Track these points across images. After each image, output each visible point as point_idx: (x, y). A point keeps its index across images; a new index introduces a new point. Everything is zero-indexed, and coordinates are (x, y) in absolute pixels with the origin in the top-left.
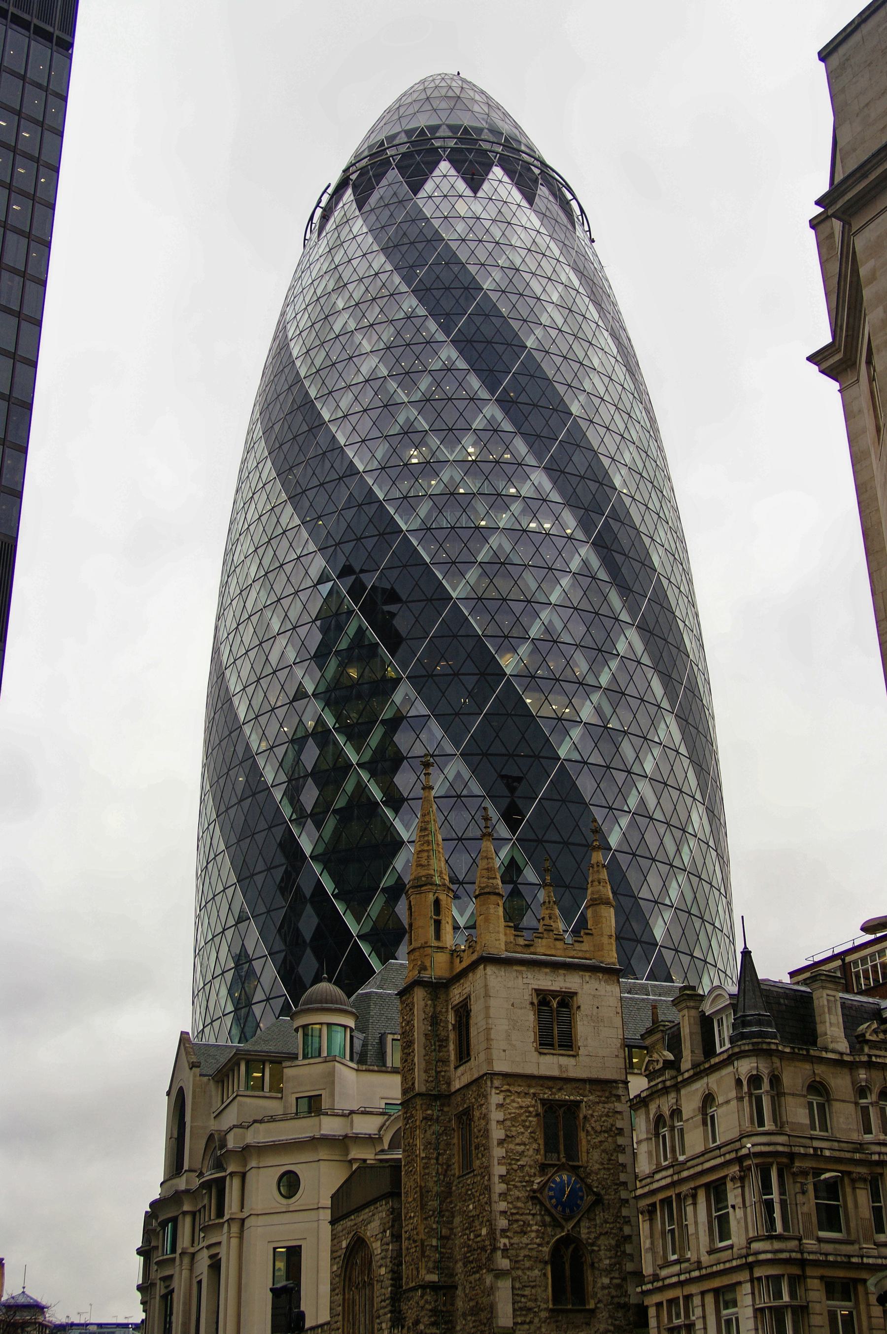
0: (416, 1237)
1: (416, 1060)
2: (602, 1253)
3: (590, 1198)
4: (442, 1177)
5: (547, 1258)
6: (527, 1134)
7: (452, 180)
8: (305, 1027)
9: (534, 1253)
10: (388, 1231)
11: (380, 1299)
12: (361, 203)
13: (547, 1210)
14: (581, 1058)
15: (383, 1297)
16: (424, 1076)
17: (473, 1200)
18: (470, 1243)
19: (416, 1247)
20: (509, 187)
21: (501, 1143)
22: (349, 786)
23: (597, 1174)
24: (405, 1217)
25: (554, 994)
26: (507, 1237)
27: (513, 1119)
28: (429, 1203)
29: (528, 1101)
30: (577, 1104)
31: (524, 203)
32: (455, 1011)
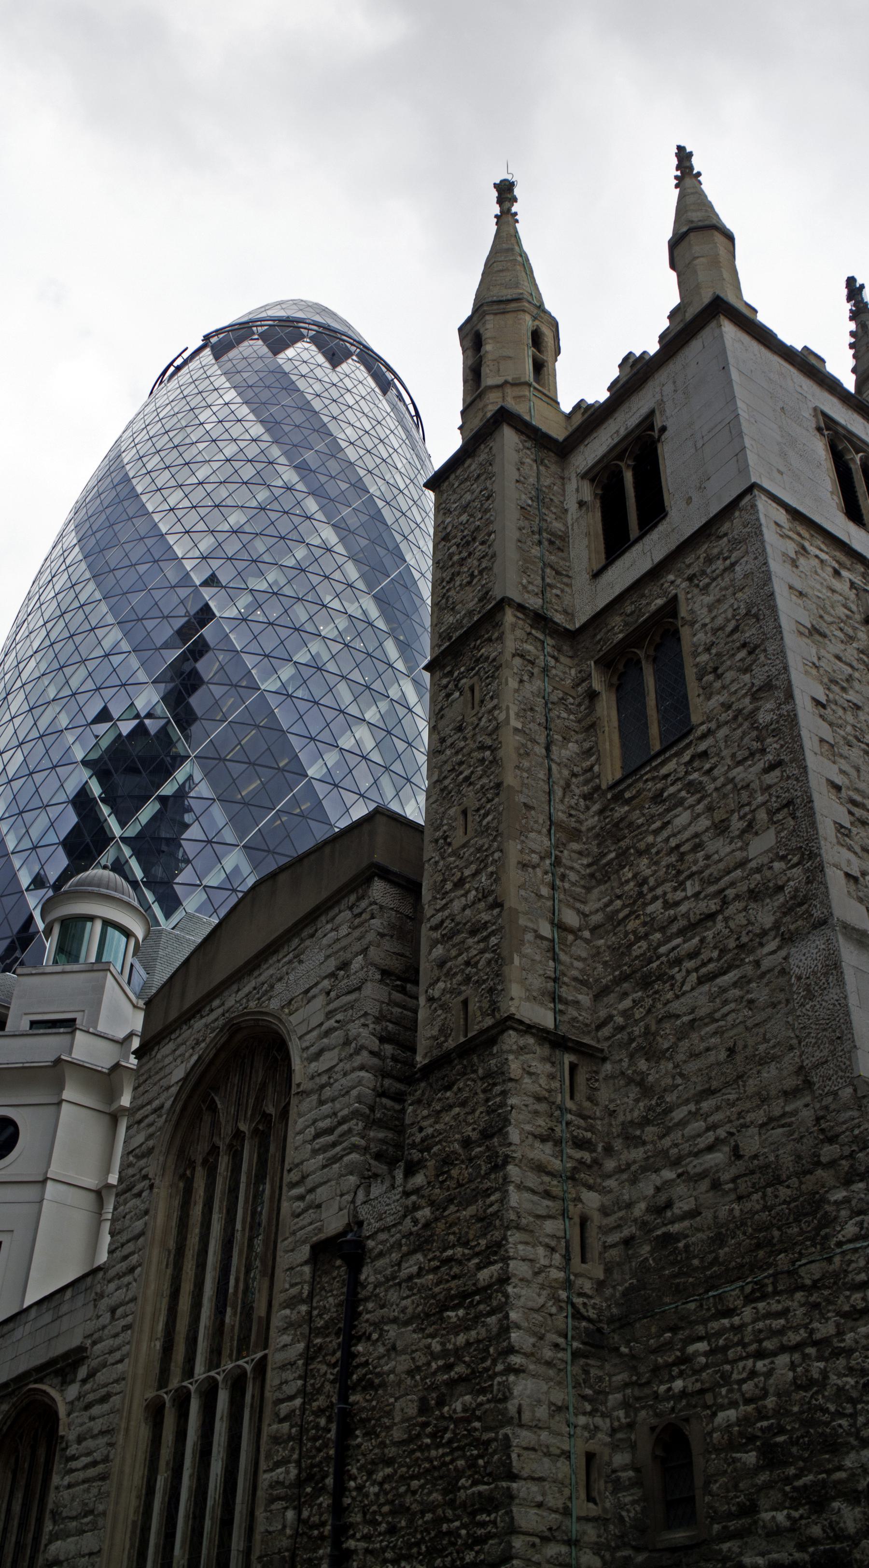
0: (485, 917)
4: (559, 792)
12: (217, 356)
17: (691, 800)
18: (683, 908)
19: (486, 939)
20: (366, 375)
28: (532, 835)
31: (377, 390)
32: (592, 480)
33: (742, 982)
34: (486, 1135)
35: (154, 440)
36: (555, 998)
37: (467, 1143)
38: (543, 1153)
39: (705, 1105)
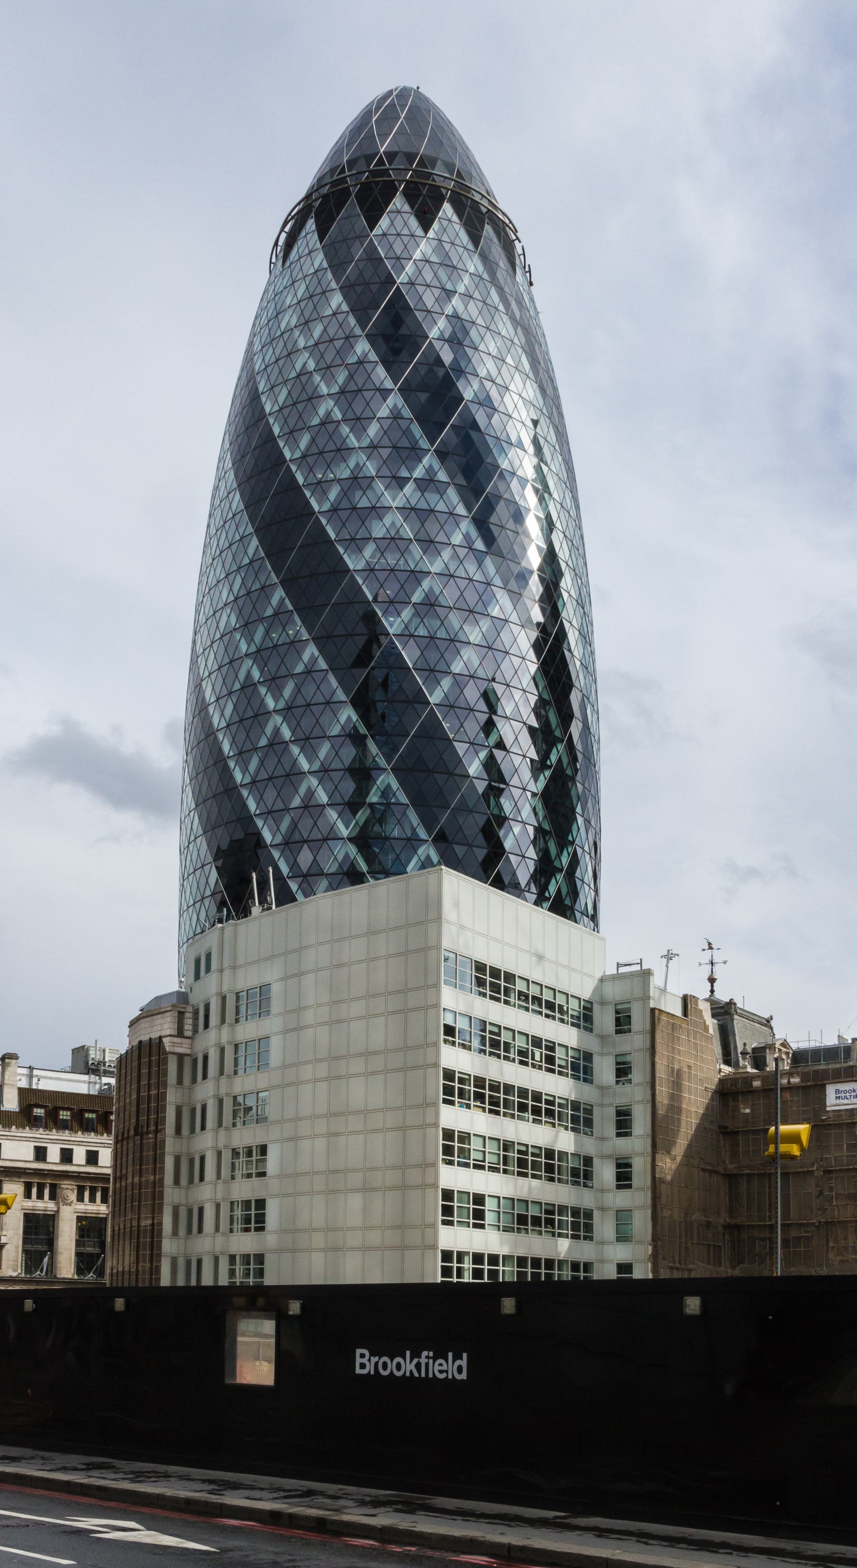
7: (405, 216)
20: (457, 227)
31: (471, 247)
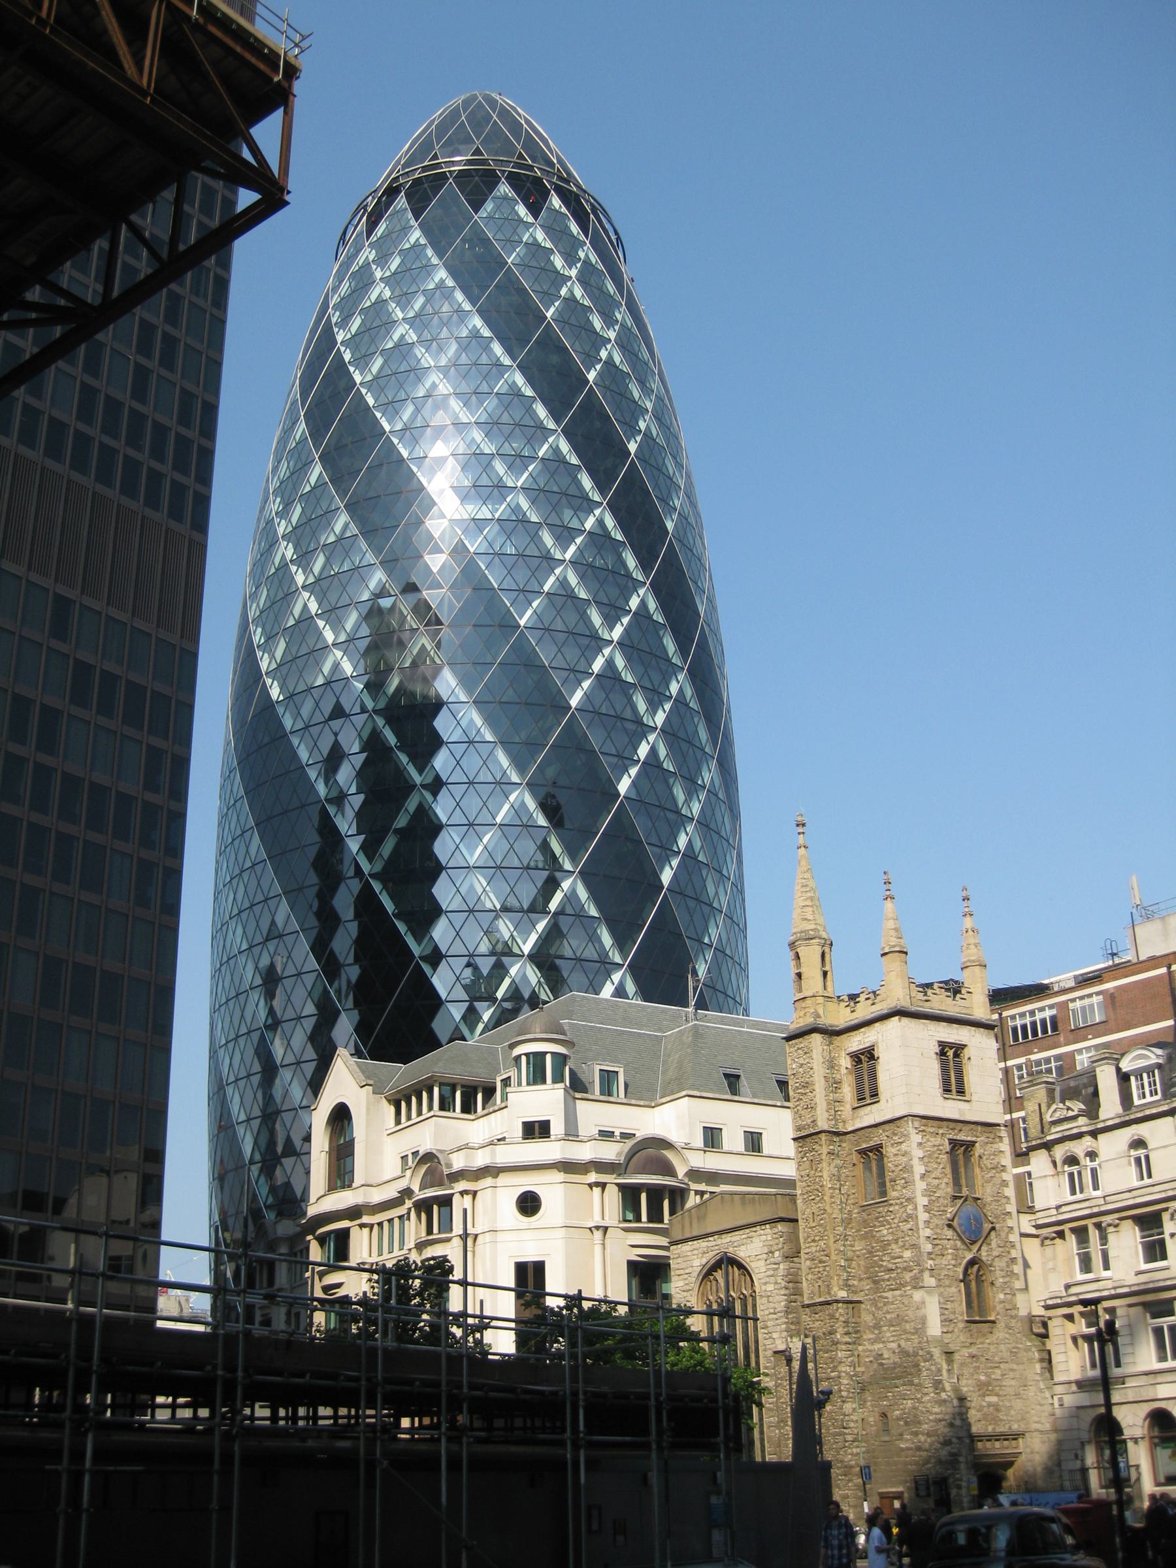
0: (824, 1258)
1: (817, 1100)
2: (998, 1272)
3: (987, 1226)
5: (961, 1277)
6: (939, 1170)
8: (527, 1055)
9: (951, 1273)
10: (777, 1254)
11: (767, 1312)
13: (959, 1235)
14: (974, 1103)
15: (772, 1311)
16: (826, 1115)
21: (923, 1177)
22: (412, 805)
23: (990, 1205)
24: (805, 1240)
25: (951, 1045)
26: (932, 1259)
27: (930, 1156)
29: (938, 1141)
30: (973, 1143)
33: (902, 1296)
34: (830, 1333)
35: (373, 332)
36: (847, 1285)
37: (824, 1334)
38: (847, 1339)
39: (892, 1329)
